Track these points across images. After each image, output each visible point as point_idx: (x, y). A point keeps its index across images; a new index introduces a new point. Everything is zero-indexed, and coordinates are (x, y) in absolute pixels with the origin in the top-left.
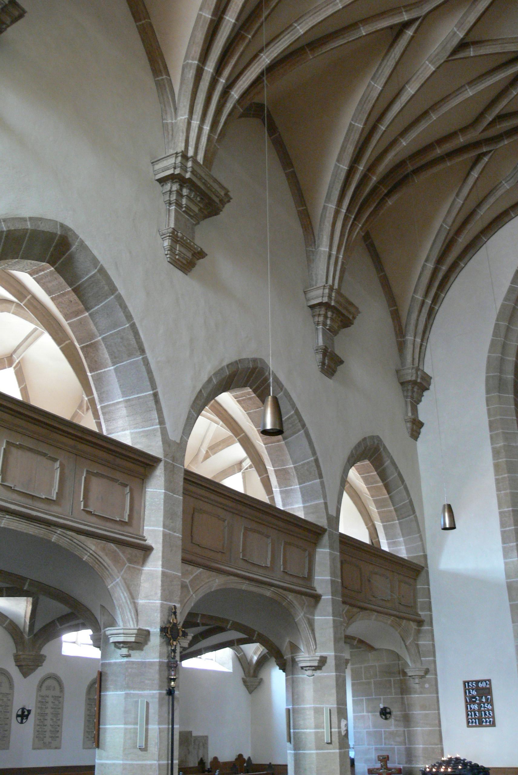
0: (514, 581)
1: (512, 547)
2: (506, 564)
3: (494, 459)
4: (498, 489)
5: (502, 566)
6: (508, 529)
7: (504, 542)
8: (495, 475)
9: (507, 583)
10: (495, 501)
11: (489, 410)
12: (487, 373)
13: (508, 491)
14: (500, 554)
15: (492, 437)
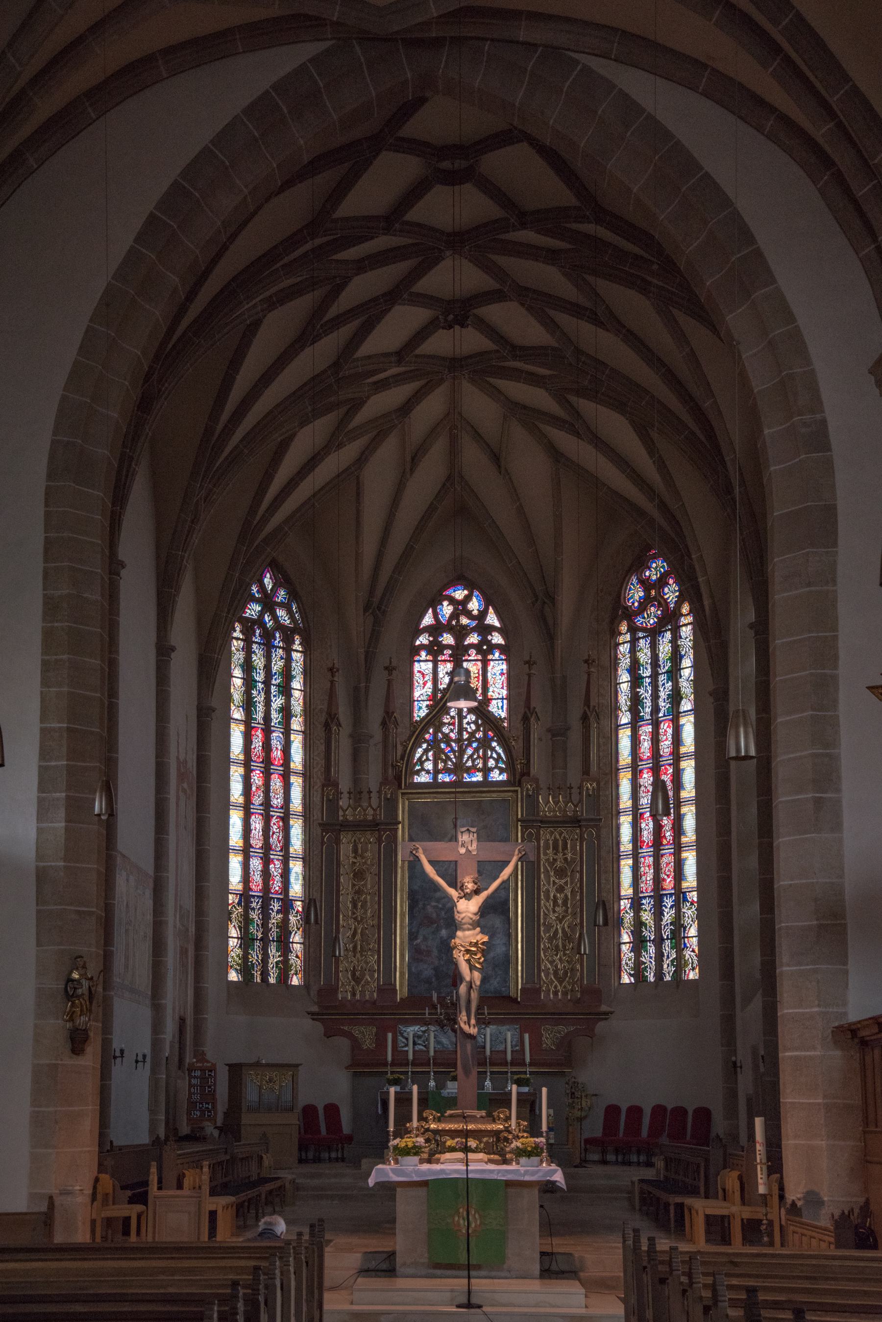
0: (51, 866)
1: (58, 799)
2: (40, 831)
3: (44, 620)
4: (45, 682)
5: (33, 834)
6: (53, 763)
7: (42, 788)
8: (44, 653)
9: (37, 867)
10: (35, 705)
11: (47, 515)
12: (54, 434)
13: (65, 689)
14: (32, 810)
15: (46, 574)
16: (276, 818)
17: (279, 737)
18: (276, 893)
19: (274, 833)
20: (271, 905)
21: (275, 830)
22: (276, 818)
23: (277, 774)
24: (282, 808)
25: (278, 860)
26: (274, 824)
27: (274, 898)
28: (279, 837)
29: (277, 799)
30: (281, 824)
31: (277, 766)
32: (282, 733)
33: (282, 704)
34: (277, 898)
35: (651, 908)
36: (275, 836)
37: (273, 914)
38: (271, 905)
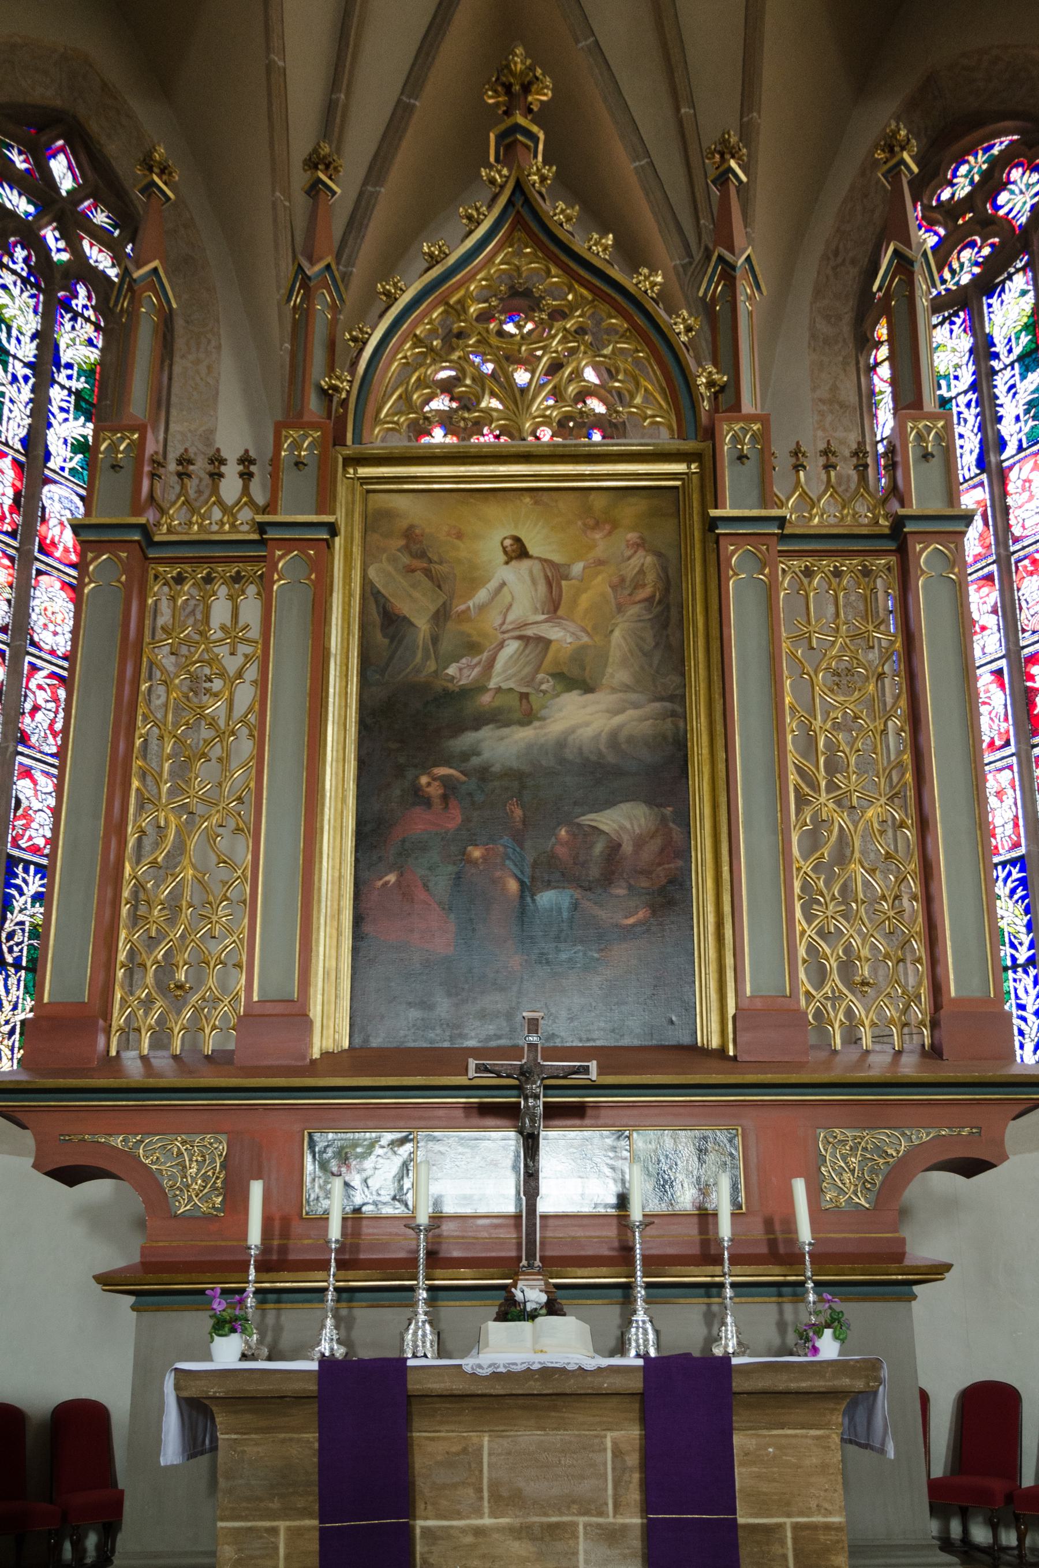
16: (49, 676)
17: (71, 501)
18: (35, 849)
19: (36, 708)
20: (16, 876)
21: (40, 702)
22: (49, 676)
23: (58, 578)
24: (65, 658)
25: (47, 774)
26: (40, 687)
27: (27, 864)
28: (53, 722)
29: (55, 634)
30: (62, 693)
31: (61, 562)
32: (82, 498)
33: (85, 437)
34: (35, 864)
35: (1013, 891)
36: (39, 716)
37: (18, 903)
38: (16, 876)
